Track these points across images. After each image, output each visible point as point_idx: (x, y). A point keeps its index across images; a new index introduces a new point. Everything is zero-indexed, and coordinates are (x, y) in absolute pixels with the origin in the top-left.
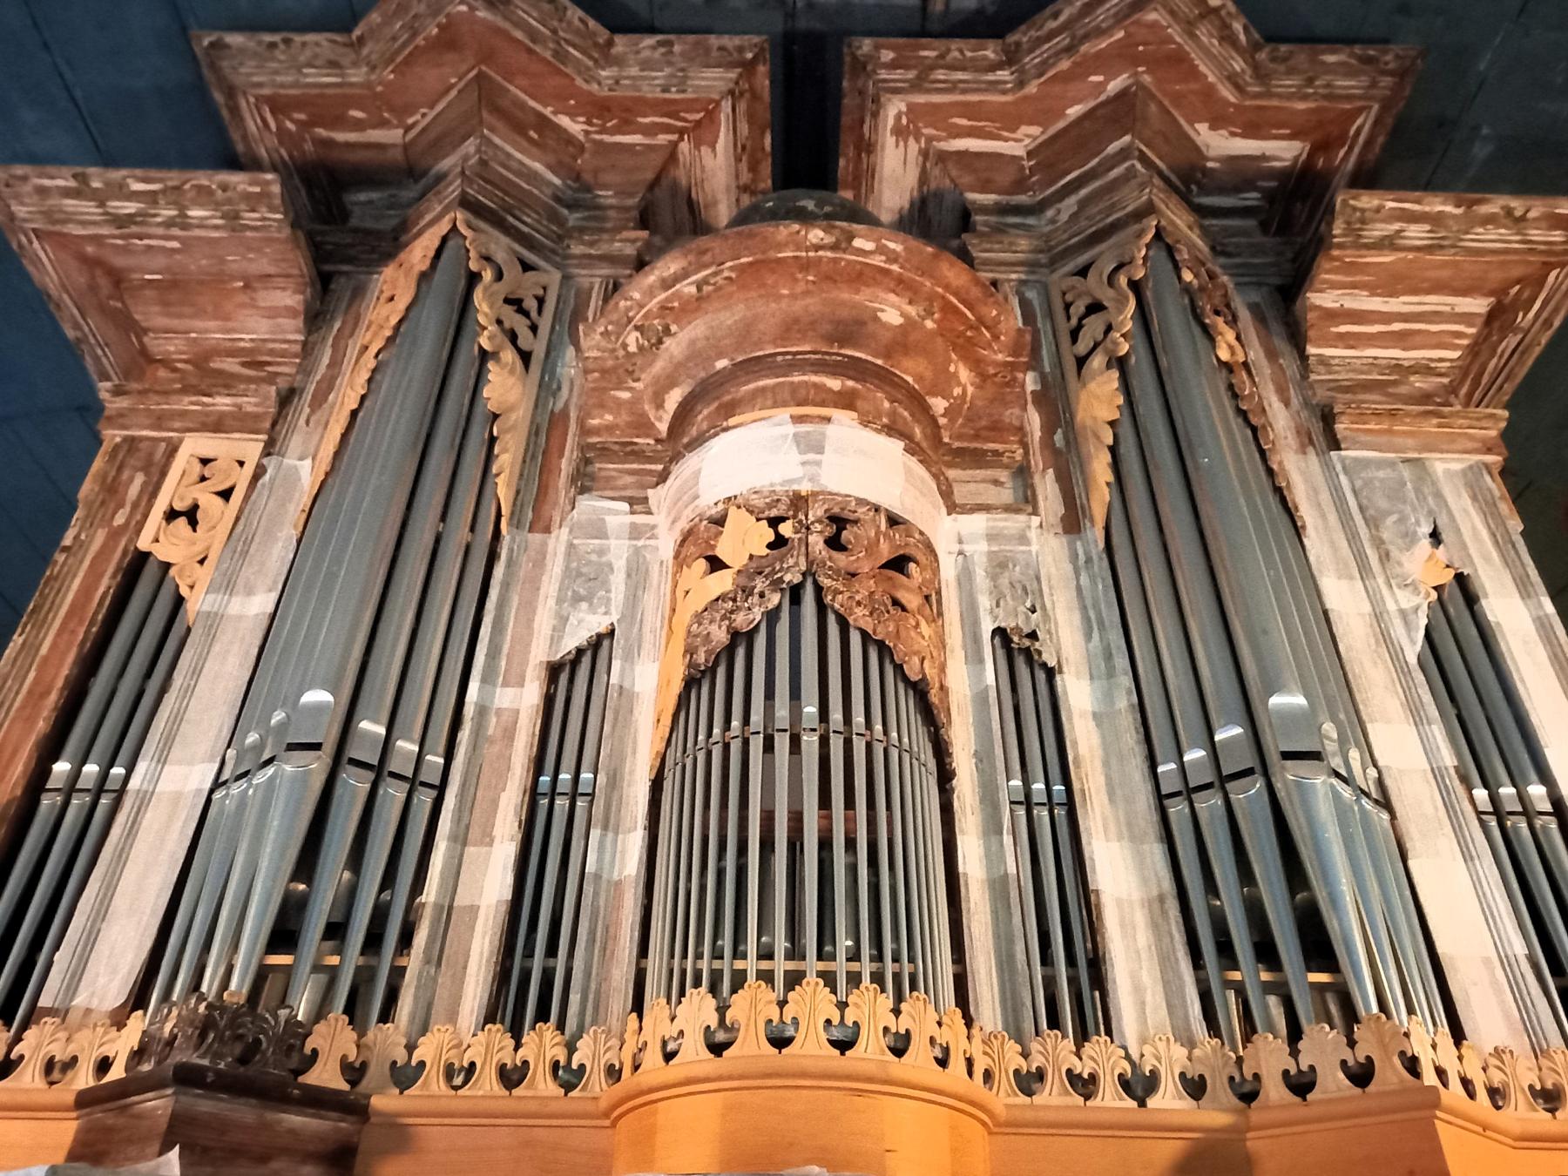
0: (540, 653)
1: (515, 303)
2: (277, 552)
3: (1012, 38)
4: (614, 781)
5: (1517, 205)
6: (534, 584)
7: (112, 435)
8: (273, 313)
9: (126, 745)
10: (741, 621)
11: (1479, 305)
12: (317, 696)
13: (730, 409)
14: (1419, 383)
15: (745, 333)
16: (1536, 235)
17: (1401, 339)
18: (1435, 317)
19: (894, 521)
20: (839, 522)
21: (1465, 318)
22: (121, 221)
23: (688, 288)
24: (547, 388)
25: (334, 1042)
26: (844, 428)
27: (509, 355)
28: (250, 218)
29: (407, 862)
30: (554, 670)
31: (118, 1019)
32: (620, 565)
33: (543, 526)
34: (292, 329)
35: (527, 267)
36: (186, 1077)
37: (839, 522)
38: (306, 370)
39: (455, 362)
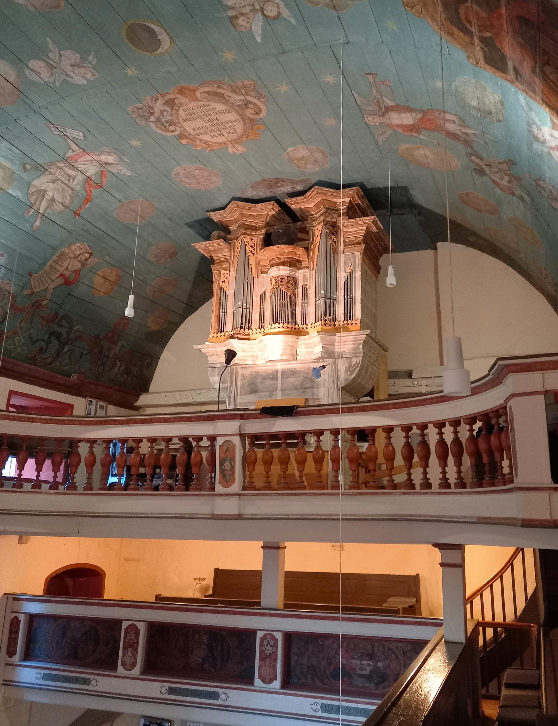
1: (251, 246)
5: (361, 219)
8: (226, 252)
11: (365, 228)
13: (272, 266)
14: (358, 239)
15: (272, 256)
16: (365, 221)
19: (288, 277)
26: (282, 267)
30: (261, 296)
35: (252, 239)
37: (282, 279)
38: (231, 259)
39: (246, 260)
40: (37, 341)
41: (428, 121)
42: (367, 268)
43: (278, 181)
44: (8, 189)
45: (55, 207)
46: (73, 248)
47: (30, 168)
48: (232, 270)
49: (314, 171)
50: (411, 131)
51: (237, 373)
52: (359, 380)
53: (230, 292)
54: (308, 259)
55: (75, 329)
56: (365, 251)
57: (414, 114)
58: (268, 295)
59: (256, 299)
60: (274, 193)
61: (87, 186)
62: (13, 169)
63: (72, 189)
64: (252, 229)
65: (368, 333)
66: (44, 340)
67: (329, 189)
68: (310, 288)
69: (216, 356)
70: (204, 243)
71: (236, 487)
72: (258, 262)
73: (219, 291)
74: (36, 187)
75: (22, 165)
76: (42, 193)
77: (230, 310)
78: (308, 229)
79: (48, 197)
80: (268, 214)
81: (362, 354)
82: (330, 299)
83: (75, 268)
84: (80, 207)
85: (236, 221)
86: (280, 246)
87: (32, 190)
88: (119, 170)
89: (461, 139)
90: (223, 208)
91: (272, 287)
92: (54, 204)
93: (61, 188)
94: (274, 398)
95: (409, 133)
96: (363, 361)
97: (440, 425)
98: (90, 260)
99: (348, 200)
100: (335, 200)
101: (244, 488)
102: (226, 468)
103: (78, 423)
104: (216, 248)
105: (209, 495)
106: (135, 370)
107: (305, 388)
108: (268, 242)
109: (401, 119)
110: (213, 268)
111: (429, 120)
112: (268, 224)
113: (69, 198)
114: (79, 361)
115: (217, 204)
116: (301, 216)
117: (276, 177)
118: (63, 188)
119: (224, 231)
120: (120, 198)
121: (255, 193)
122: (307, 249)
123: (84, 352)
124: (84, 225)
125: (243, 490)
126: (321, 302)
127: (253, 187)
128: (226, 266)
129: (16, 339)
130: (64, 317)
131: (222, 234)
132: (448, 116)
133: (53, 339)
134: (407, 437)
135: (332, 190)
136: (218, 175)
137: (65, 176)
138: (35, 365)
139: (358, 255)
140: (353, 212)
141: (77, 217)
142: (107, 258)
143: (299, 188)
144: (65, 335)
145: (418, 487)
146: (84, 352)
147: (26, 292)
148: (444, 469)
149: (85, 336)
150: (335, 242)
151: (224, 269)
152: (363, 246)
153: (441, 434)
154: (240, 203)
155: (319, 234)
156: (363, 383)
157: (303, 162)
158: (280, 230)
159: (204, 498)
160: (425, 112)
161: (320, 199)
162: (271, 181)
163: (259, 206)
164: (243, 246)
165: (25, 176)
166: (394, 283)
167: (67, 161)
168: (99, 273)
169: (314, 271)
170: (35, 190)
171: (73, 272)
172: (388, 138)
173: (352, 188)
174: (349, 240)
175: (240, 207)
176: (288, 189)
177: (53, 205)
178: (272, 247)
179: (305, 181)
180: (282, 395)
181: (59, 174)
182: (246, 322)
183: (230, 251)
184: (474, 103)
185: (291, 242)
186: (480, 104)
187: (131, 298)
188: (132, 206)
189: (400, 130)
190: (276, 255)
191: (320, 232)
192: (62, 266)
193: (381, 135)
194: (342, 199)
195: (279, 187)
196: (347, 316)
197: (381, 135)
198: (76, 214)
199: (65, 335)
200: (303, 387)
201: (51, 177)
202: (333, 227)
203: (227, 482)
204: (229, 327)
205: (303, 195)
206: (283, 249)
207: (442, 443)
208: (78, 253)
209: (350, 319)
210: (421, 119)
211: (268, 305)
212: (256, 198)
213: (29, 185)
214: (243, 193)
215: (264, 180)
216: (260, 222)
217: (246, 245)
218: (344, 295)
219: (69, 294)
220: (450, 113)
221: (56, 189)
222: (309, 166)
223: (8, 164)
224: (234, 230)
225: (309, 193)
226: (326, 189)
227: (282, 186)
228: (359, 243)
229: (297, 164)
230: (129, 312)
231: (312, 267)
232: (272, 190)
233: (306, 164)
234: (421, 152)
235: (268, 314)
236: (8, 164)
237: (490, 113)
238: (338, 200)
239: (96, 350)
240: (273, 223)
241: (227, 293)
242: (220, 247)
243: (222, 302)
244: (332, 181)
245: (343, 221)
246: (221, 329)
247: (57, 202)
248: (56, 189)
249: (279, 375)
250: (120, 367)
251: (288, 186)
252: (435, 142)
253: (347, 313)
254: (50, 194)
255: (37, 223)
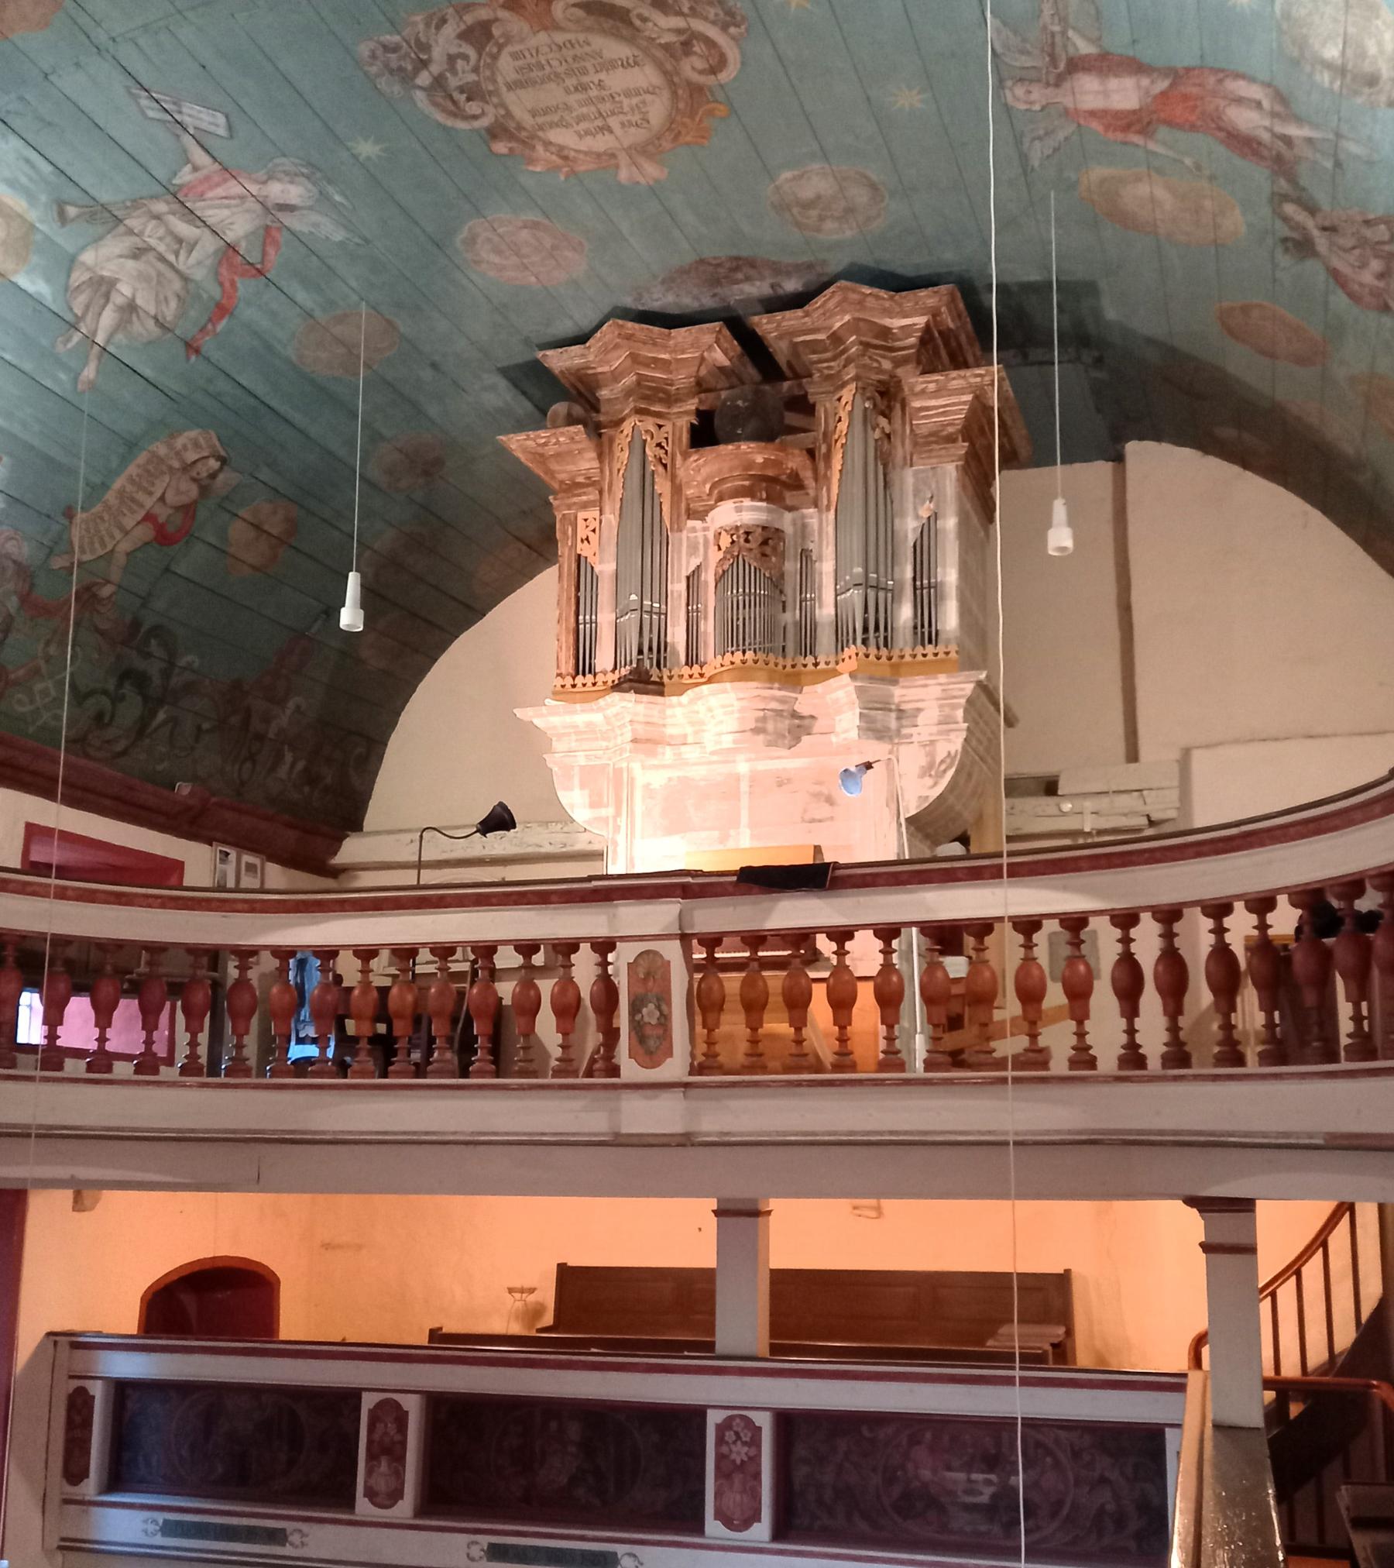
0: (685, 573)
1: (659, 445)
2: (612, 549)
3: (806, 308)
4: (706, 607)
6: (680, 552)
7: (559, 517)
9: (594, 610)
10: (726, 567)
11: (969, 397)
12: (633, 597)
13: (721, 499)
14: (951, 429)
15: (720, 471)
16: (973, 380)
17: (943, 414)
18: (954, 404)
19: (764, 528)
20: (747, 533)
21: (964, 403)
22: (539, 445)
23: (701, 461)
24: (673, 477)
25: (654, 672)
26: (747, 502)
27: (661, 469)
28: (577, 438)
29: (663, 632)
30: (688, 578)
31: (613, 671)
32: (701, 541)
33: (680, 530)
34: (596, 464)
35: (660, 426)
36: (631, 680)
37: (747, 533)
39: (645, 479)
40: (91, 693)
41: (1184, 100)
42: (968, 506)
43: (741, 266)
44: (16, 272)
45: (136, 327)
46: (179, 442)
47: (78, 217)
48: (607, 508)
49: (840, 240)
50: (1127, 128)
51: (632, 781)
52: (951, 799)
53: (606, 568)
54: (816, 480)
55: (182, 662)
56: (967, 462)
57: (1145, 82)
58: (709, 577)
59: (678, 588)
60: (723, 300)
61: (224, 271)
62: (33, 215)
63: (185, 279)
64: (661, 400)
65: (983, 676)
66: (105, 692)
67: (876, 290)
68: (820, 558)
69: (574, 737)
70: (532, 434)
71: (675, 1068)
72: (677, 490)
73: (574, 566)
74: (88, 269)
75: (55, 208)
76: (104, 287)
77: (605, 618)
78: (811, 399)
79: (117, 299)
80: (702, 359)
81: (964, 734)
82: (877, 588)
83: (184, 500)
84: (203, 330)
85: (616, 376)
86: (744, 447)
87: (78, 277)
88: (316, 225)
89: (1266, 153)
90: (581, 339)
91: (721, 555)
92: (134, 318)
93: (154, 274)
94: (731, 844)
95: (1120, 136)
96: (964, 748)
97: (1218, 910)
98: (221, 477)
99: (921, 321)
100: (887, 322)
101: (697, 1069)
102: (646, 1019)
103: (246, 906)
104: (564, 448)
105: (605, 1087)
106: (329, 776)
107: (813, 821)
108: (704, 433)
109: (1106, 94)
110: (555, 503)
111: (1186, 97)
112: (701, 387)
113: (173, 304)
114: (193, 748)
115: (565, 328)
116: (790, 365)
117: (734, 253)
118: (159, 274)
119: (581, 402)
120: (309, 304)
121: (670, 298)
122: (811, 453)
123: (206, 726)
124: (210, 381)
125: (690, 1074)
126: (855, 595)
127: (669, 282)
128: (591, 497)
129: (38, 687)
130: (156, 631)
131: (578, 410)
132: (1241, 88)
133: (128, 689)
134: (1126, 941)
135: (883, 293)
136: (580, 243)
137: (168, 239)
138: (87, 756)
139: (949, 474)
140: (939, 351)
141: (193, 358)
142: (265, 474)
143: (791, 285)
144: (157, 680)
145: (1154, 1064)
146: (206, 726)
147: (58, 563)
148: (1227, 1017)
149: (207, 682)
150: (888, 436)
151: (585, 506)
152: (962, 448)
153: (1220, 931)
154: (630, 324)
155: (844, 415)
156: (958, 808)
157: (814, 213)
158: (740, 403)
159: (590, 1094)
160: (1177, 75)
161: (847, 318)
162: (719, 265)
163: (680, 334)
164: (638, 445)
165: (65, 240)
166: (1069, 543)
167: (174, 195)
168: (241, 512)
169: (832, 511)
170: (86, 276)
171: (177, 508)
172: (1056, 150)
173: (936, 289)
174: (924, 431)
175: (629, 337)
176: (758, 288)
177: (130, 322)
178: (722, 447)
179: (810, 266)
180: (753, 837)
181: (152, 234)
182: (650, 649)
183: (600, 457)
184: (1332, 52)
185: (767, 435)
186: (1349, 52)
187: (353, 580)
188: (337, 330)
189: (1096, 125)
190: (731, 470)
191: (849, 408)
192: (151, 494)
193: (1040, 138)
194: (907, 319)
195: (737, 282)
196: (923, 633)
197: (1040, 138)
198: (191, 347)
199: (157, 680)
200: (807, 818)
201: (128, 242)
202: (882, 394)
203: (650, 1053)
204: (604, 659)
205: (801, 306)
206: (756, 453)
207: (1222, 952)
208: (191, 456)
209: (930, 642)
210: (1163, 94)
211: (710, 598)
212: (675, 311)
213: (71, 262)
214: (640, 297)
215: (702, 261)
216: (682, 379)
217: (645, 441)
218: (914, 579)
219: (167, 570)
220: (1252, 79)
221: (142, 277)
222: (829, 225)
223: (17, 202)
224: (609, 400)
225: (819, 301)
226: (867, 290)
227: (748, 279)
228: (951, 439)
229: (799, 218)
230: (350, 617)
231: (825, 502)
232: (719, 290)
233: (821, 219)
234: (1143, 189)
235: (708, 627)
236: (17, 202)
237: (1372, 81)
238: (896, 323)
239: (235, 720)
240: (712, 383)
241: (596, 570)
242: (574, 446)
243: (581, 594)
244: (883, 267)
245: (914, 381)
246: (583, 665)
247: (141, 314)
248: (142, 277)
249: (744, 787)
250: (295, 767)
251: (762, 278)
252: (1188, 161)
253: (923, 626)
254: (125, 289)
255: (89, 372)
